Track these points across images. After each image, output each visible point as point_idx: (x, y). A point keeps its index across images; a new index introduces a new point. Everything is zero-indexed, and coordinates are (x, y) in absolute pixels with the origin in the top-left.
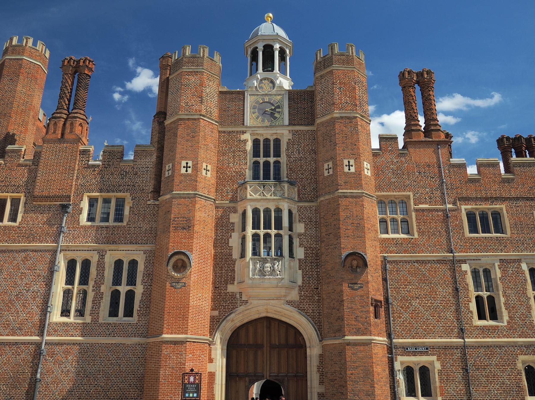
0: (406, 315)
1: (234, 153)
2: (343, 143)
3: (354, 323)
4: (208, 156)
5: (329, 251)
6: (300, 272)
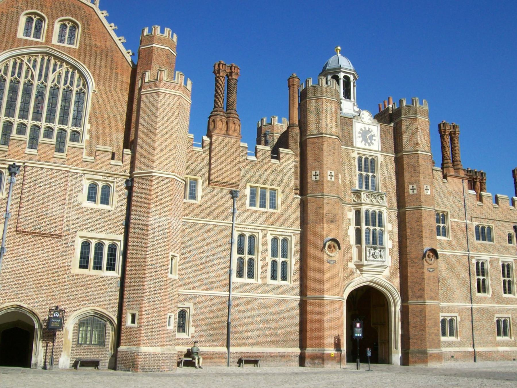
2: (424, 173)
3: (430, 293)
5: (414, 245)
6: (390, 257)
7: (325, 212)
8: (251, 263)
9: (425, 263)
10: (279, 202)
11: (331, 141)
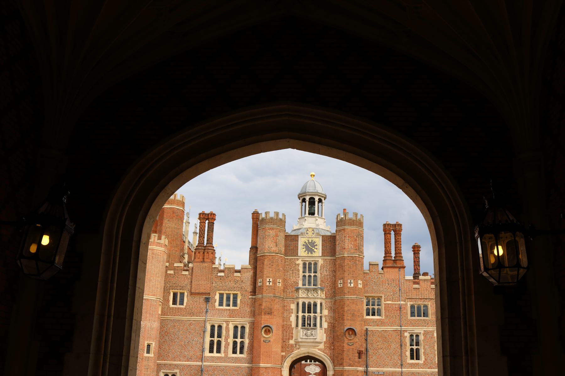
0: (374, 357)
7: (263, 307)
8: (219, 343)
9: (345, 339)
10: (239, 302)
11: (271, 257)
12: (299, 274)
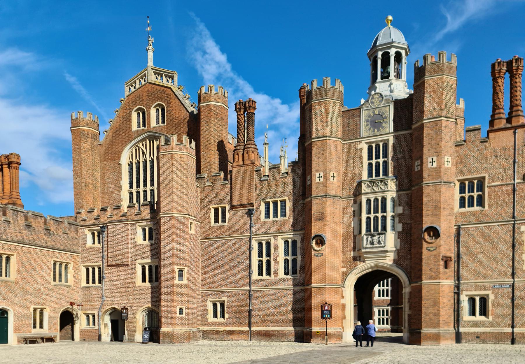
1: (354, 159)
4: (334, 166)
8: (269, 263)
12: (362, 163)
